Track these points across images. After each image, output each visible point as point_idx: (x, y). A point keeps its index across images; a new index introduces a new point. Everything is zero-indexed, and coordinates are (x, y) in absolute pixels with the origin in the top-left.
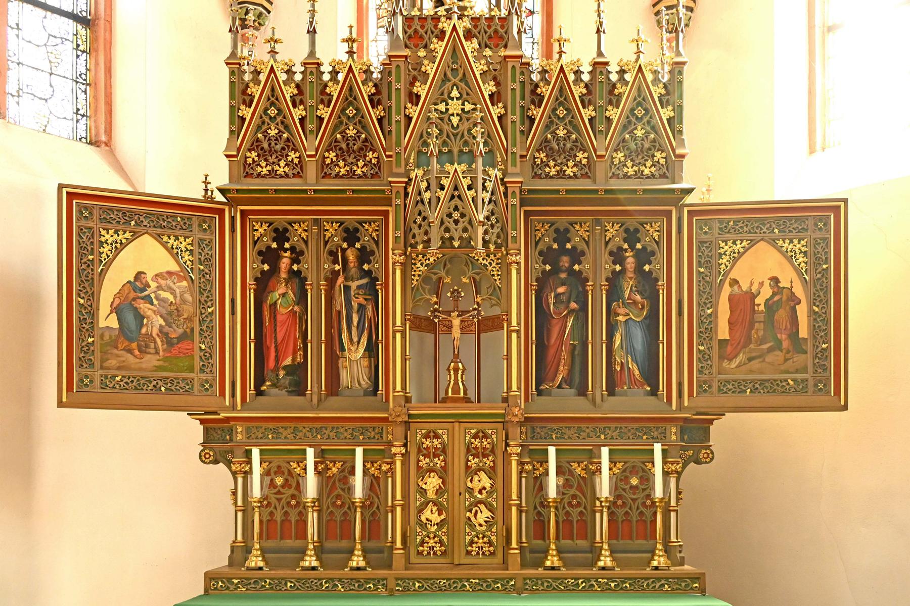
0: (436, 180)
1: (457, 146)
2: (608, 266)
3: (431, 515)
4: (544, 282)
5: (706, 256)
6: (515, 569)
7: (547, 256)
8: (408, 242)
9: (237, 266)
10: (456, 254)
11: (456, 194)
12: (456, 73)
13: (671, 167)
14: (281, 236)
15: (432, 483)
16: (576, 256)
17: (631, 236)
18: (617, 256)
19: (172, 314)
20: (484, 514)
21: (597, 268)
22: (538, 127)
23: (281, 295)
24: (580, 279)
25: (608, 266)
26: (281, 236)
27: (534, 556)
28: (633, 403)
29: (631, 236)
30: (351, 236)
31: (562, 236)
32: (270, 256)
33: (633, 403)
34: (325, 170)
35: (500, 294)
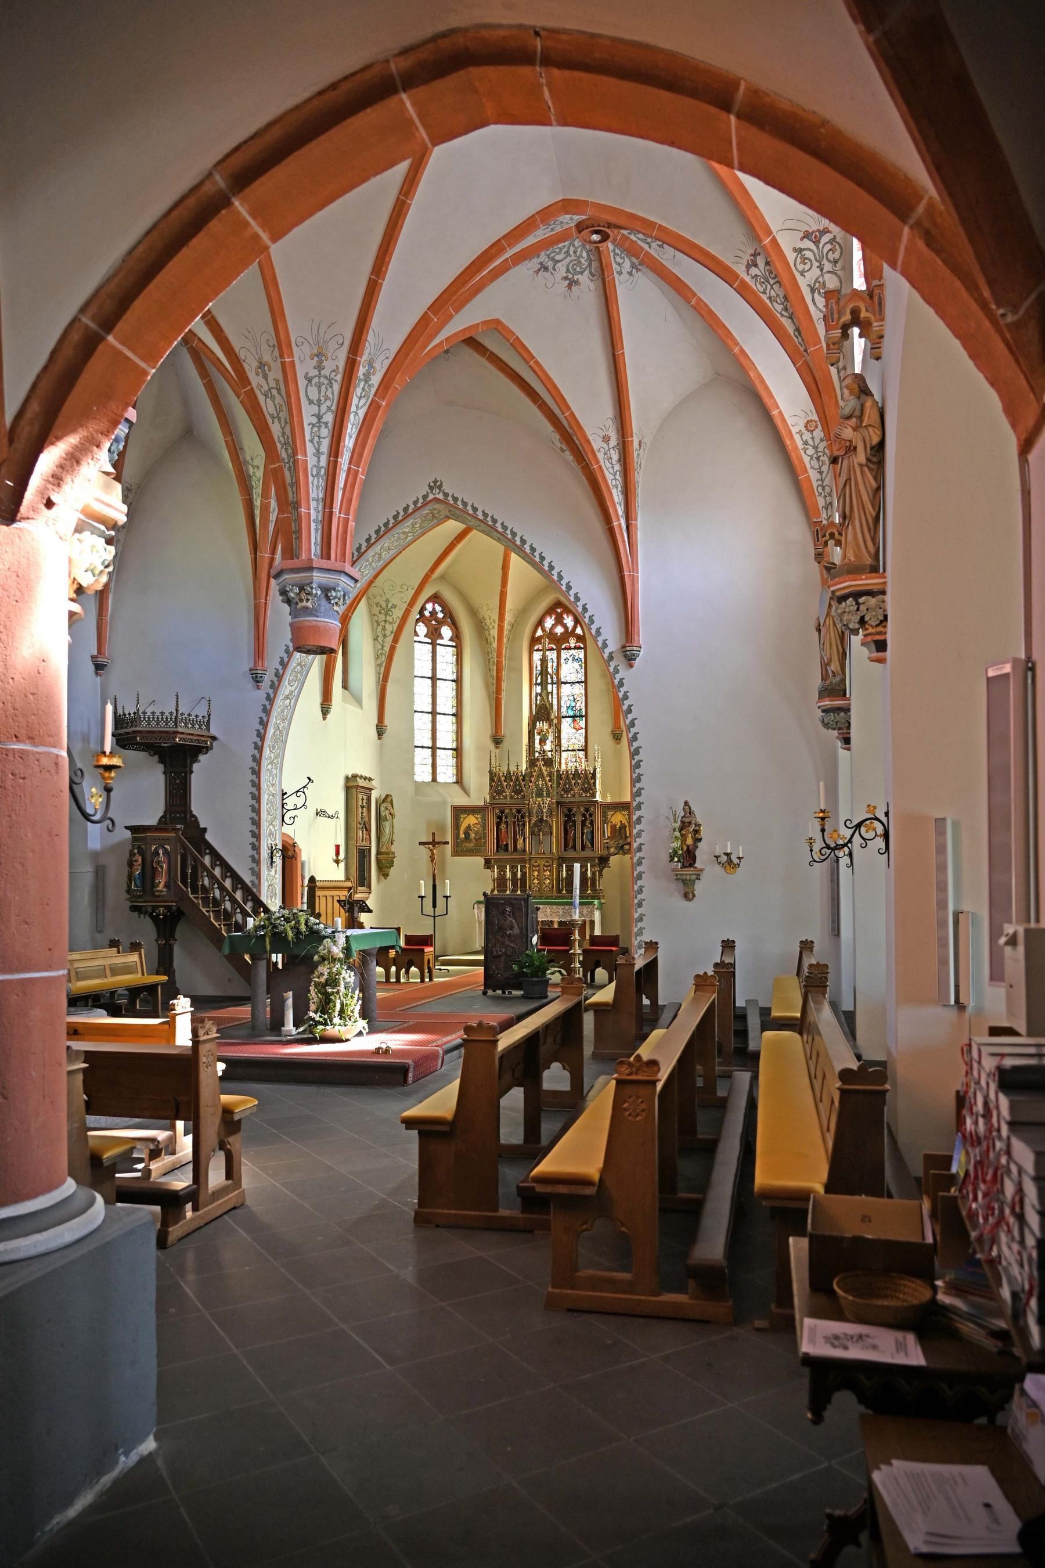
0: (534, 802)
1: (540, 794)
2: (581, 818)
3: (536, 881)
4: (566, 823)
5: (605, 816)
6: (555, 894)
7: (566, 816)
8: (529, 816)
9: (491, 821)
10: (541, 820)
11: (539, 805)
12: (541, 775)
13: (594, 795)
14: (502, 812)
15: (536, 873)
16: (574, 815)
17: (587, 810)
18: (584, 815)
19: (476, 833)
20: (548, 881)
21: (579, 819)
22: (561, 786)
23: (503, 826)
24: (574, 822)
25: (581, 818)
26: (502, 812)
27: (559, 891)
28: (587, 853)
29: (587, 810)
30: (519, 811)
31: (570, 810)
32: (500, 818)
33: (587, 853)
34: (512, 797)
35: (551, 827)
